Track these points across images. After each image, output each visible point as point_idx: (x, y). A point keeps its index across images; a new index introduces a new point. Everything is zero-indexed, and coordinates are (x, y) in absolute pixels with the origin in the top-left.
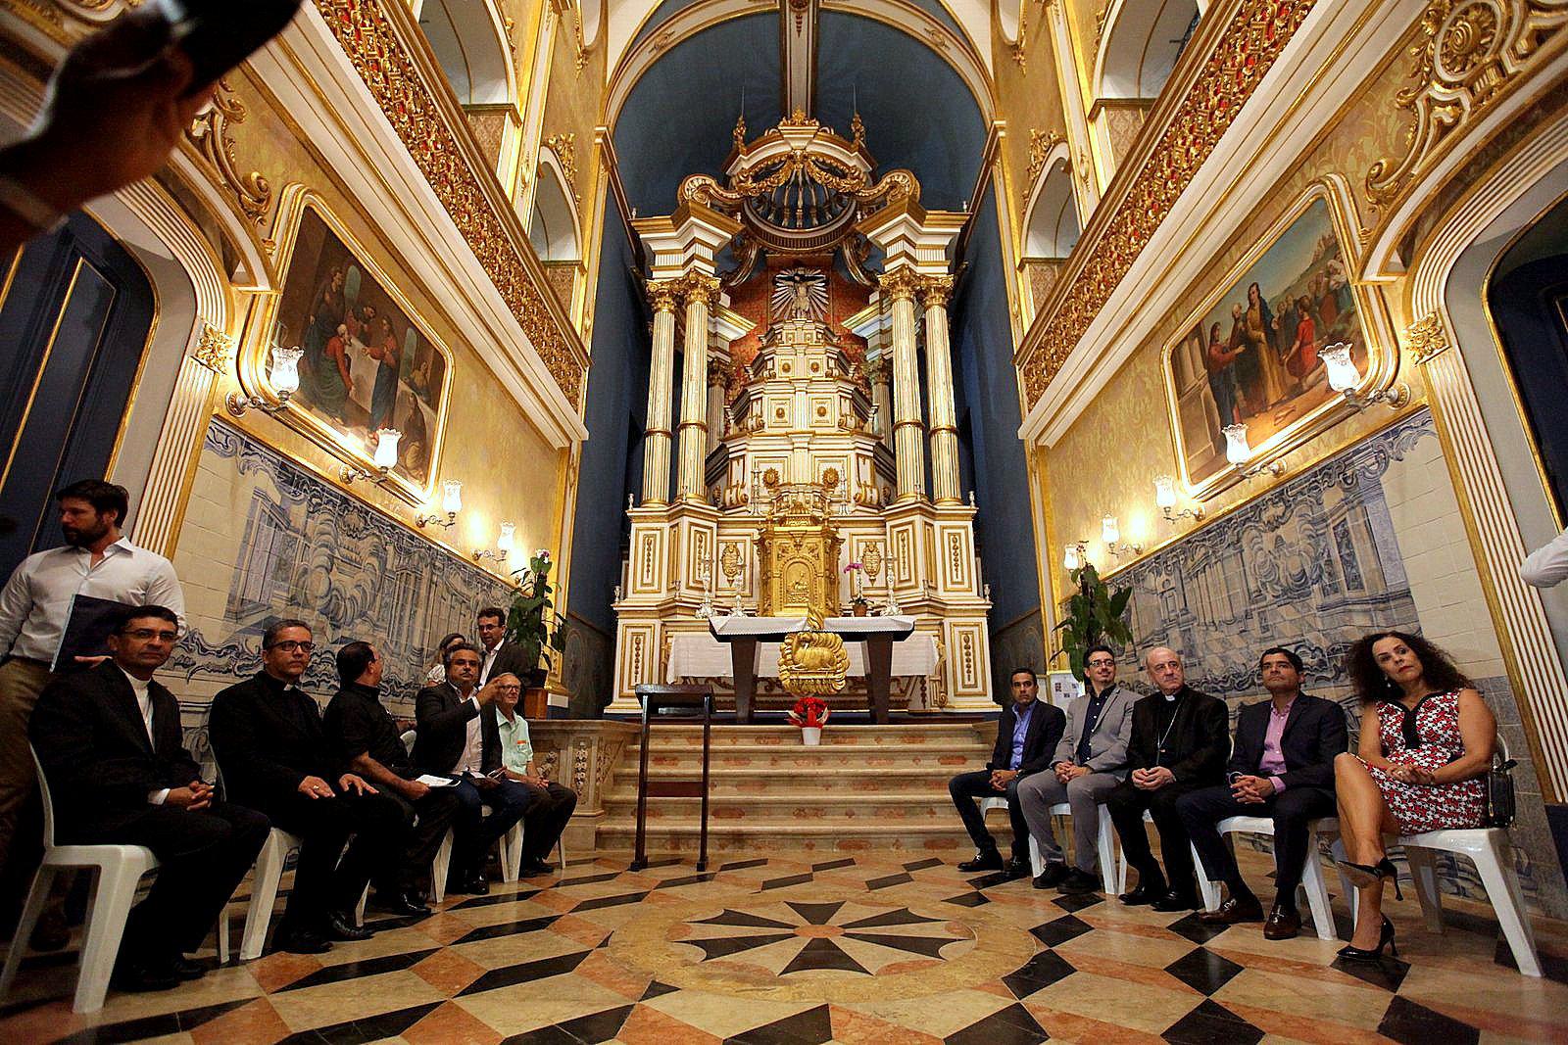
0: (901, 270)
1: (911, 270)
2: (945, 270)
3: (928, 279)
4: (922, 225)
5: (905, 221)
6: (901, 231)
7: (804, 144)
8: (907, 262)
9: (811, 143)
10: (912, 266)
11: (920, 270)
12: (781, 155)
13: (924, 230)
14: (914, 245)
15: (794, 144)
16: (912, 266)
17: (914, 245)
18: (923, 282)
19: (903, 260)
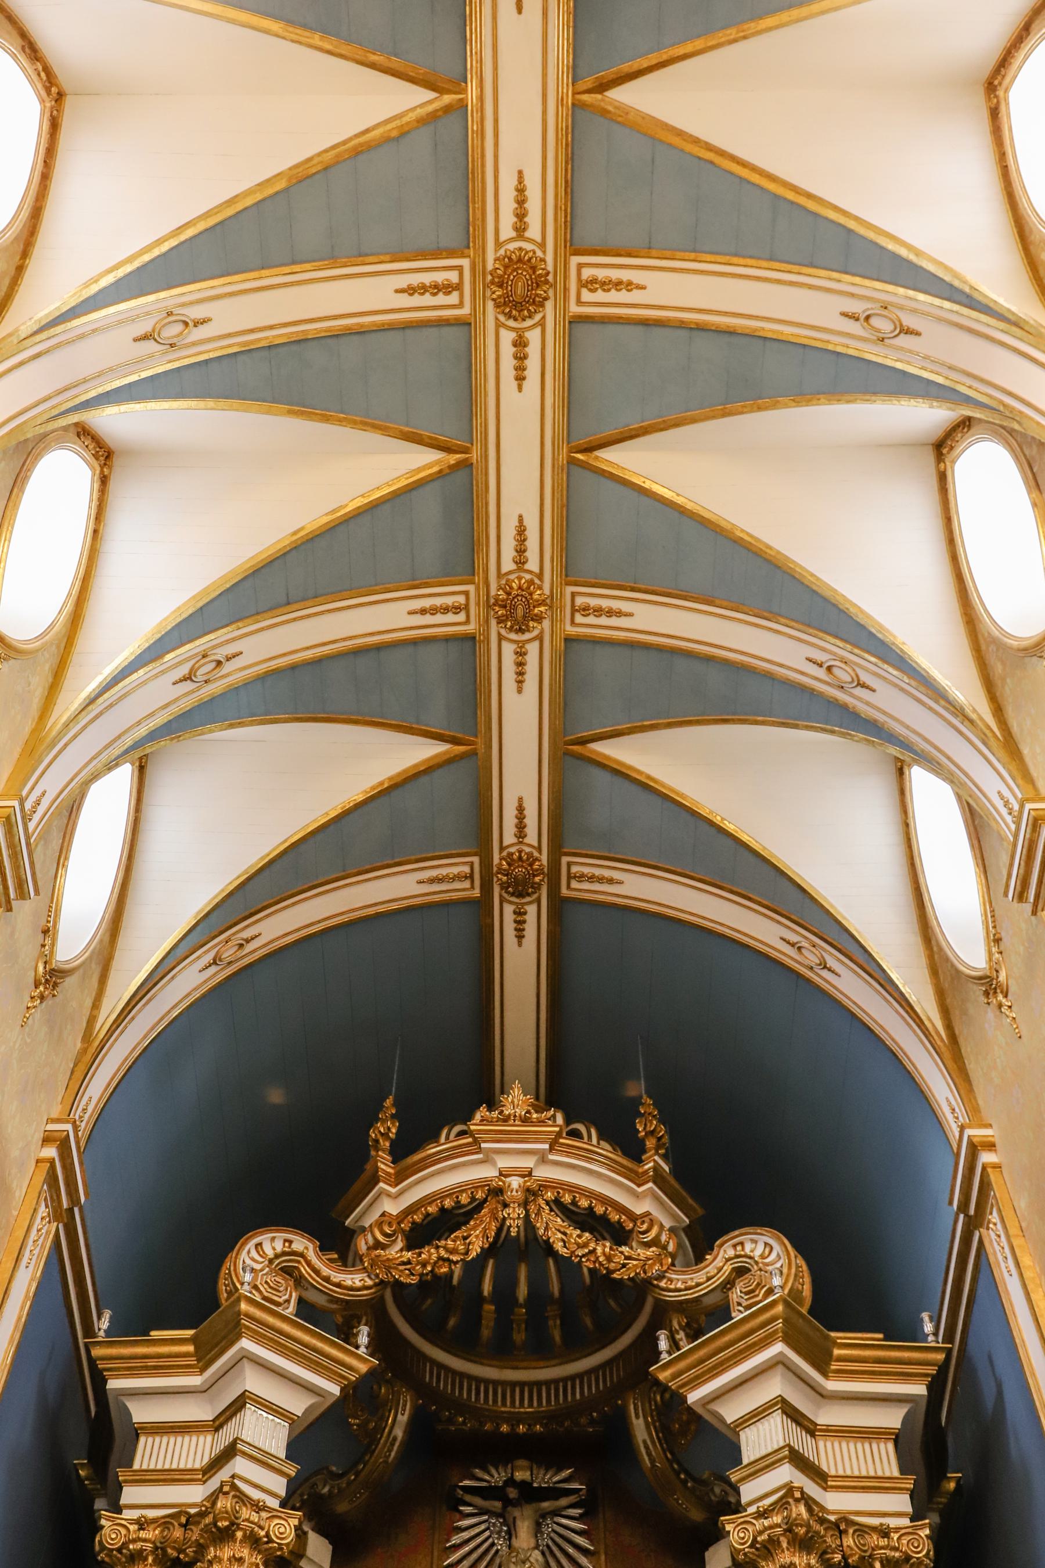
0: (782, 1504)
1: (808, 1502)
2: (902, 1502)
3: (862, 1530)
4: (825, 1374)
5: (779, 1362)
6: (774, 1387)
7: (528, 1162)
8: (800, 1480)
9: (543, 1160)
10: (812, 1489)
11: (835, 1502)
12: (476, 1185)
13: (832, 1385)
14: (811, 1429)
15: (504, 1162)
16: (812, 1489)
17: (811, 1429)
18: (849, 1541)
19: (785, 1474)
